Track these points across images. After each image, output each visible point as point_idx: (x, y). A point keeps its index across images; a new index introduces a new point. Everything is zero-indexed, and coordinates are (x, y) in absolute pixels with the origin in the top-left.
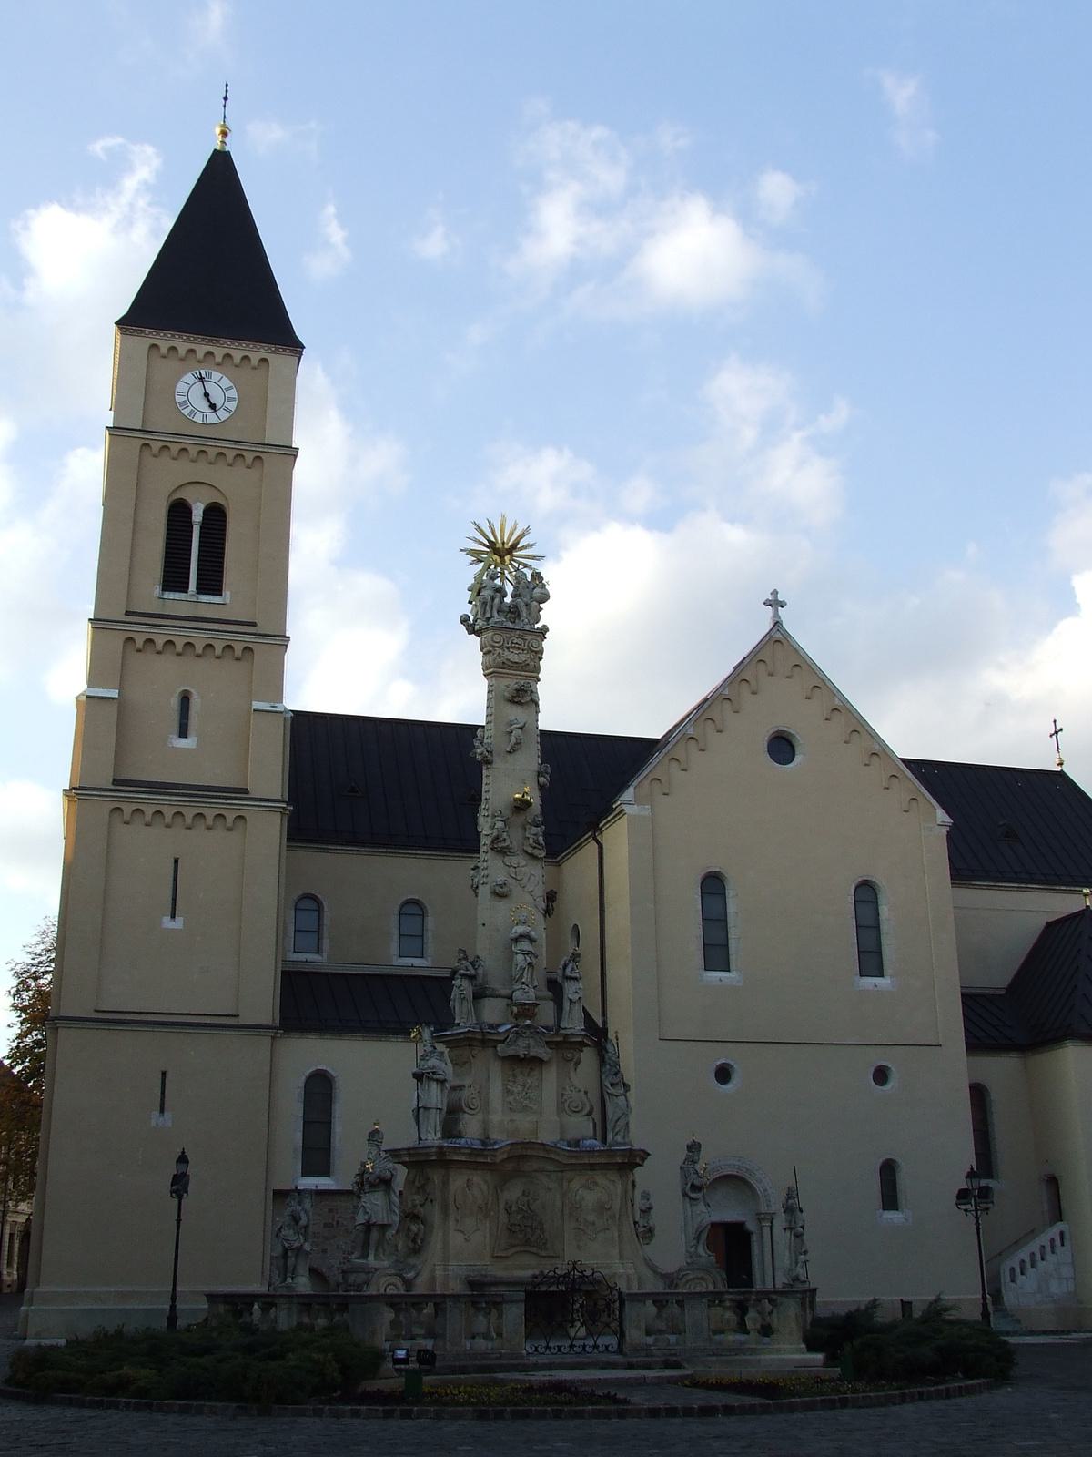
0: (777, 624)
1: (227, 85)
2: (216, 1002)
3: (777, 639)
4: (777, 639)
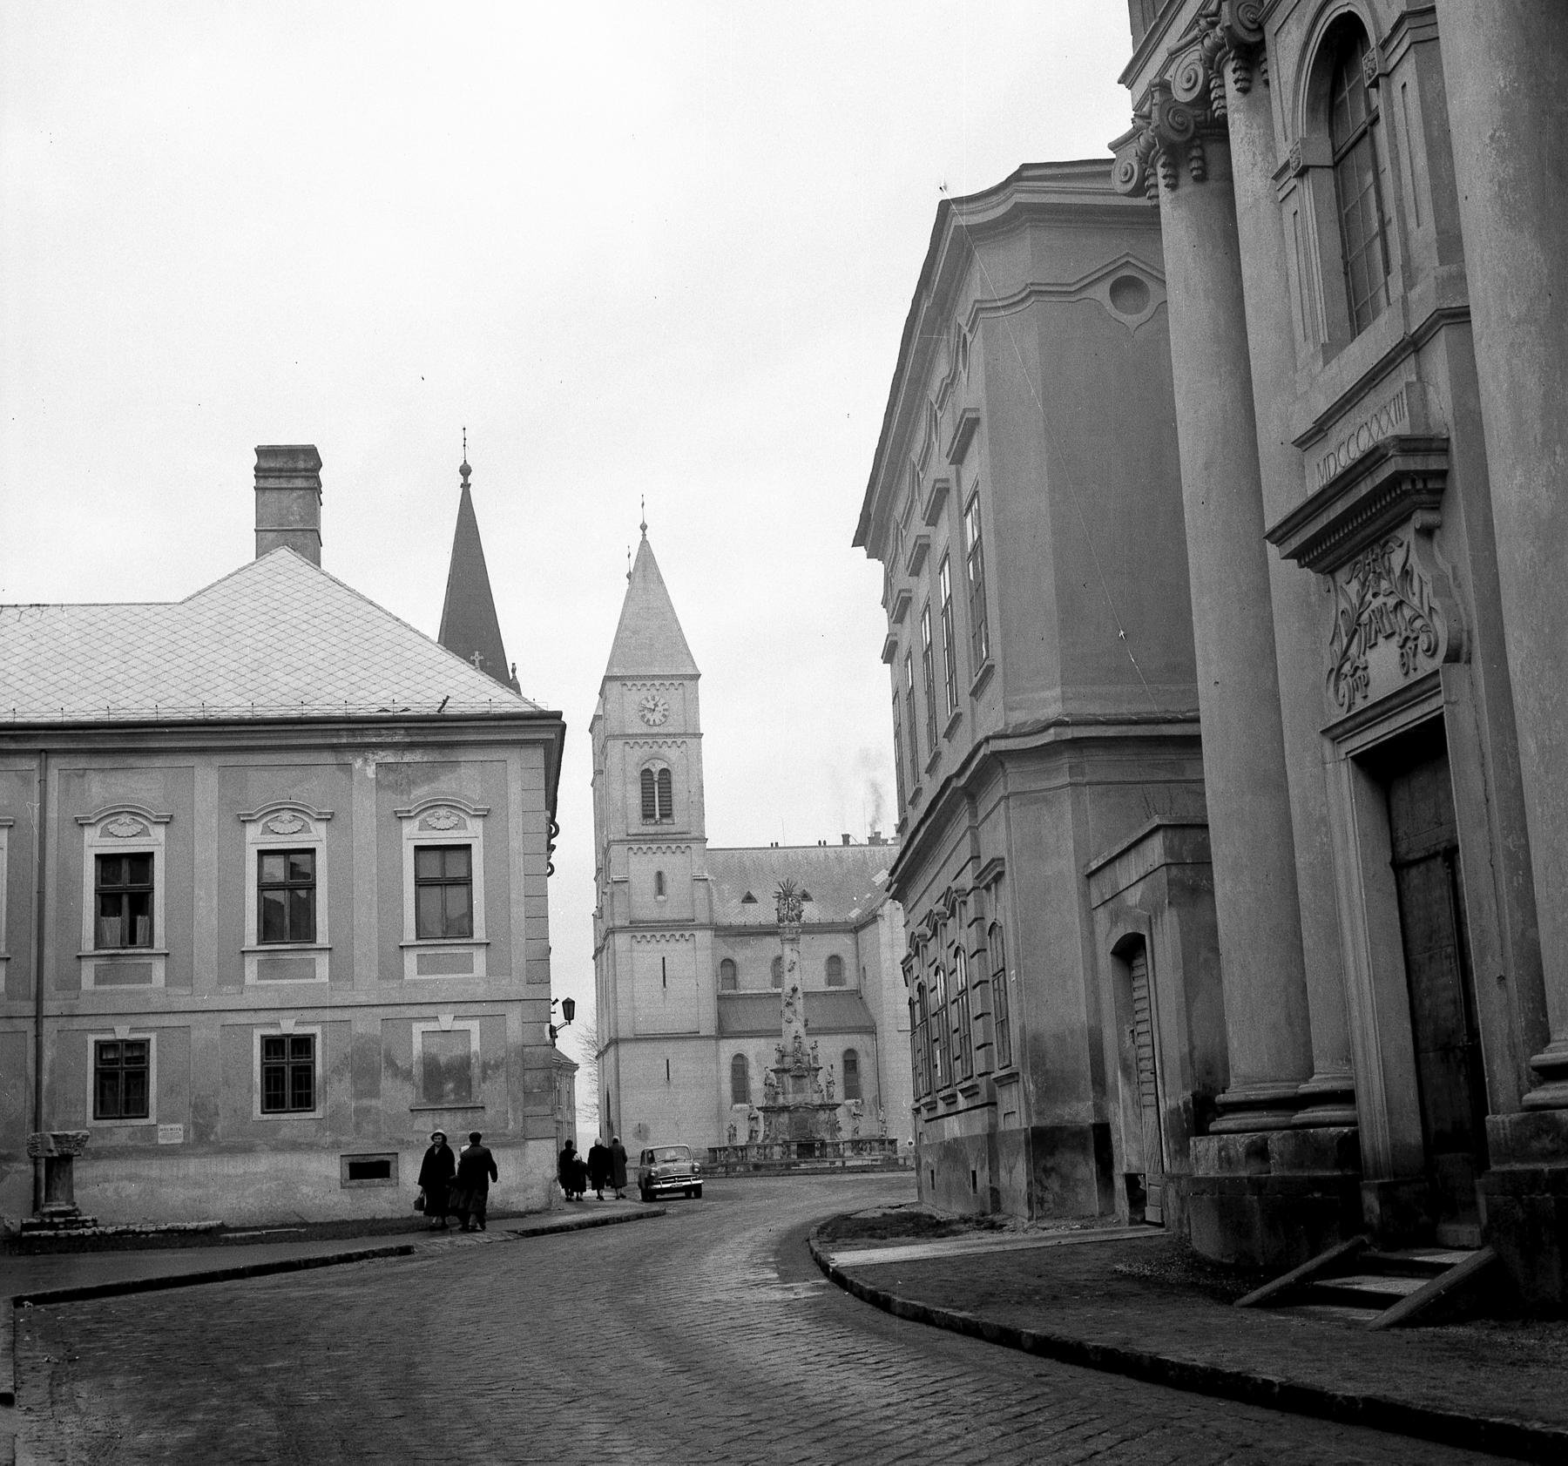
2: (688, 1027)
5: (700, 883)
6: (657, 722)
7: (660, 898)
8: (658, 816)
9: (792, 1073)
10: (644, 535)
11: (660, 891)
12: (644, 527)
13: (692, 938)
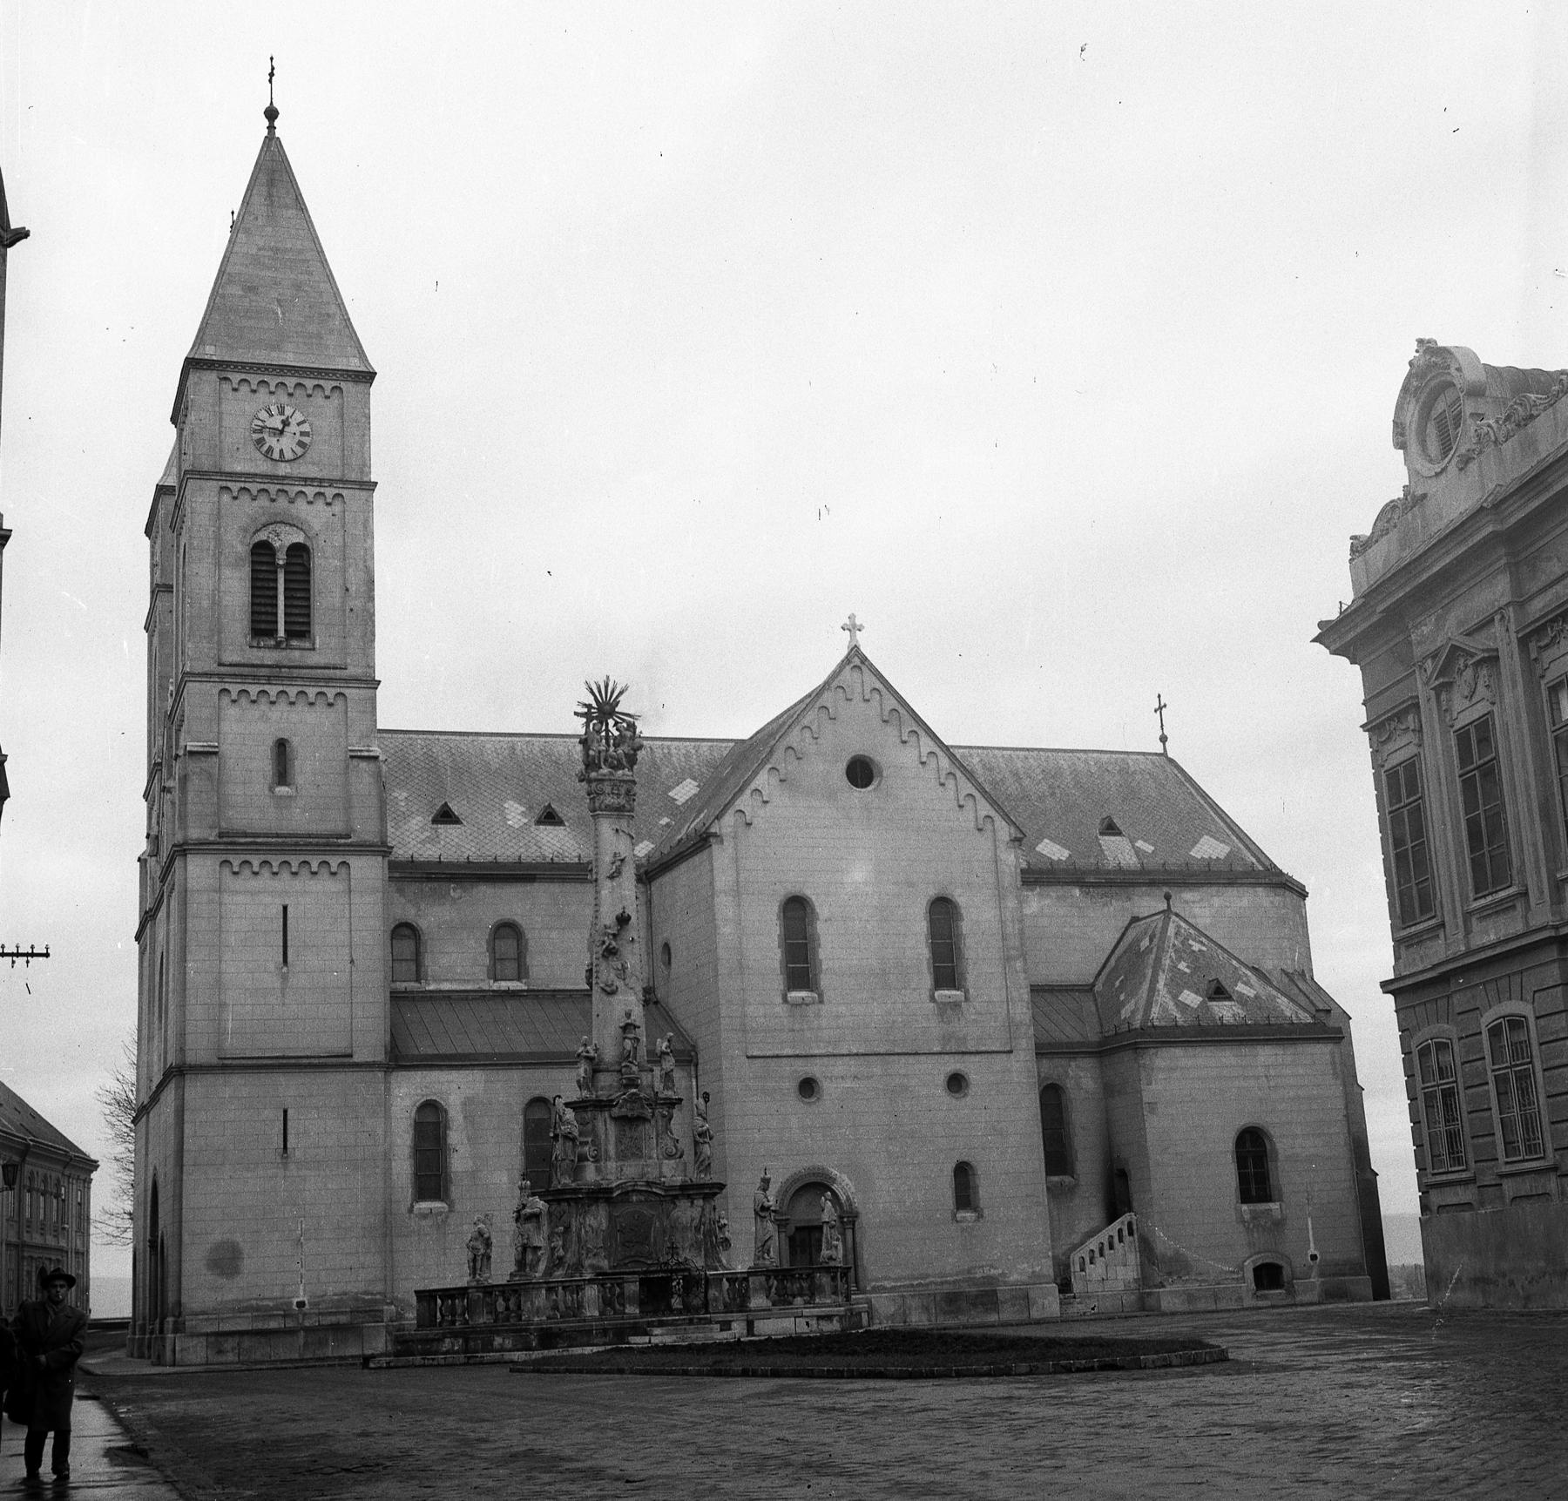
0: (855, 651)
1: (272, 59)
2: (332, 1043)
3: (856, 659)
4: (856, 659)
5: (363, 765)
6: (288, 455)
8: (281, 633)
9: (616, 1111)
10: (271, 128)
11: (282, 774)
12: (271, 114)
13: (343, 870)
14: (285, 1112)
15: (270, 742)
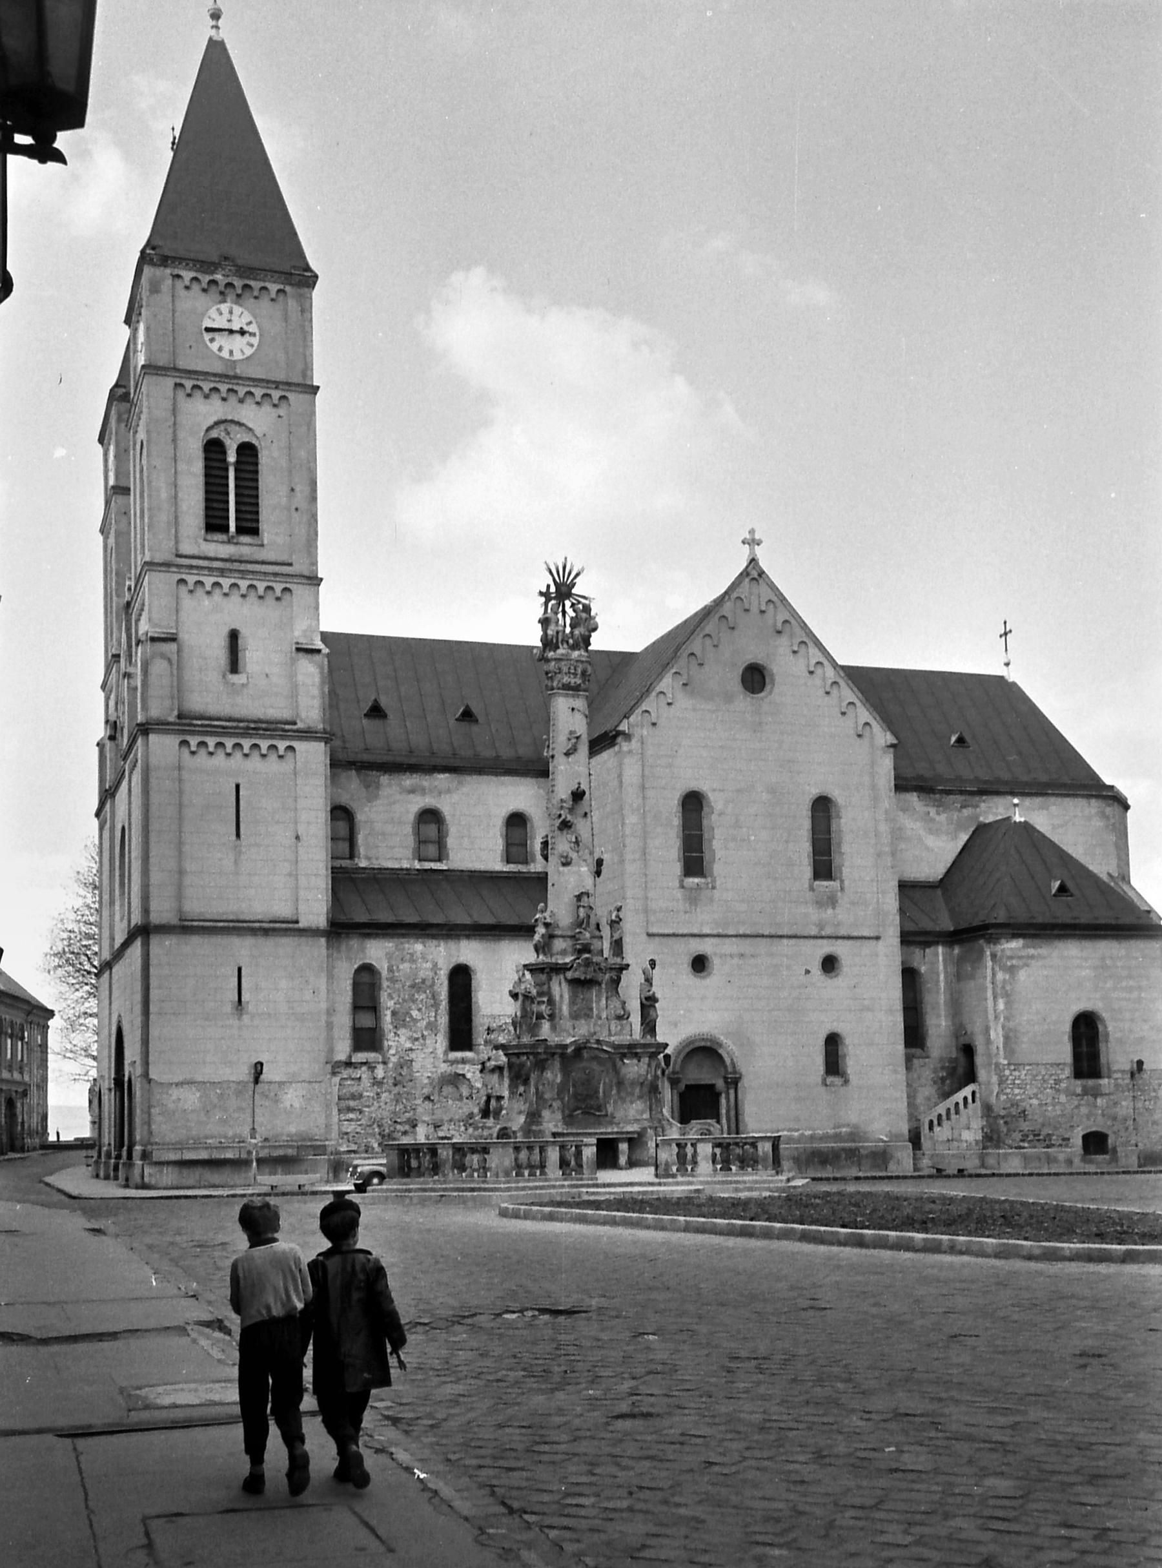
3: (753, 573)
4: (753, 573)
7: (234, 678)
11: (234, 666)
13: (290, 754)
14: (240, 970)
15: (225, 631)
